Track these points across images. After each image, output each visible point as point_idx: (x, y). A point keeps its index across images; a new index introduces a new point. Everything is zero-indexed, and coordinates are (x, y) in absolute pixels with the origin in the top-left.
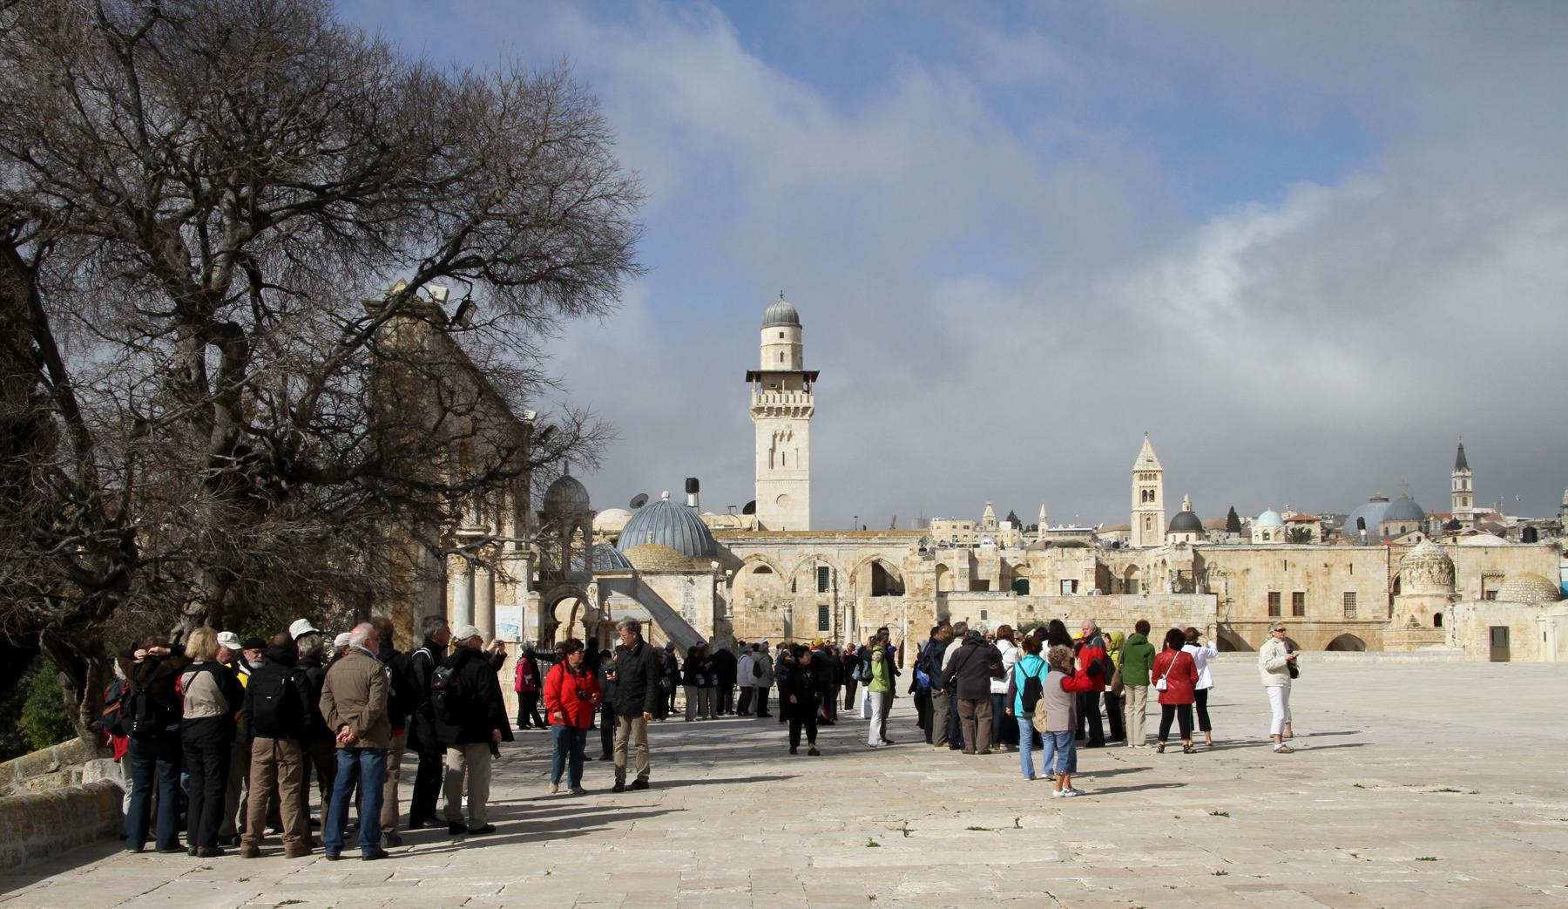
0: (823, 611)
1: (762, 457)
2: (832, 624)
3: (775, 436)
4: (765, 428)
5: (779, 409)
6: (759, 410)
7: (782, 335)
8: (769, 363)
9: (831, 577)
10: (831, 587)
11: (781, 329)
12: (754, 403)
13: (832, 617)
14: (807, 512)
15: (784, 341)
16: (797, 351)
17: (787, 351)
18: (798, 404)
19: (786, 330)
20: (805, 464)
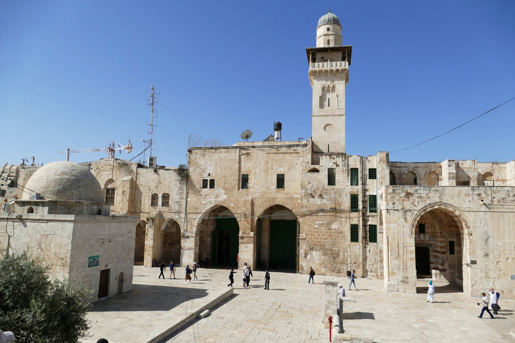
0: (354, 198)
1: (316, 101)
2: (360, 207)
3: (323, 88)
4: (317, 85)
5: (326, 71)
6: (314, 73)
7: (328, 29)
8: (320, 43)
9: (360, 175)
10: (360, 182)
11: (328, 26)
12: (311, 68)
13: (360, 203)
14: (343, 135)
15: (330, 33)
16: (337, 37)
17: (331, 38)
18: (338, 67)
19: (331, 27)
20: (343, 105)
